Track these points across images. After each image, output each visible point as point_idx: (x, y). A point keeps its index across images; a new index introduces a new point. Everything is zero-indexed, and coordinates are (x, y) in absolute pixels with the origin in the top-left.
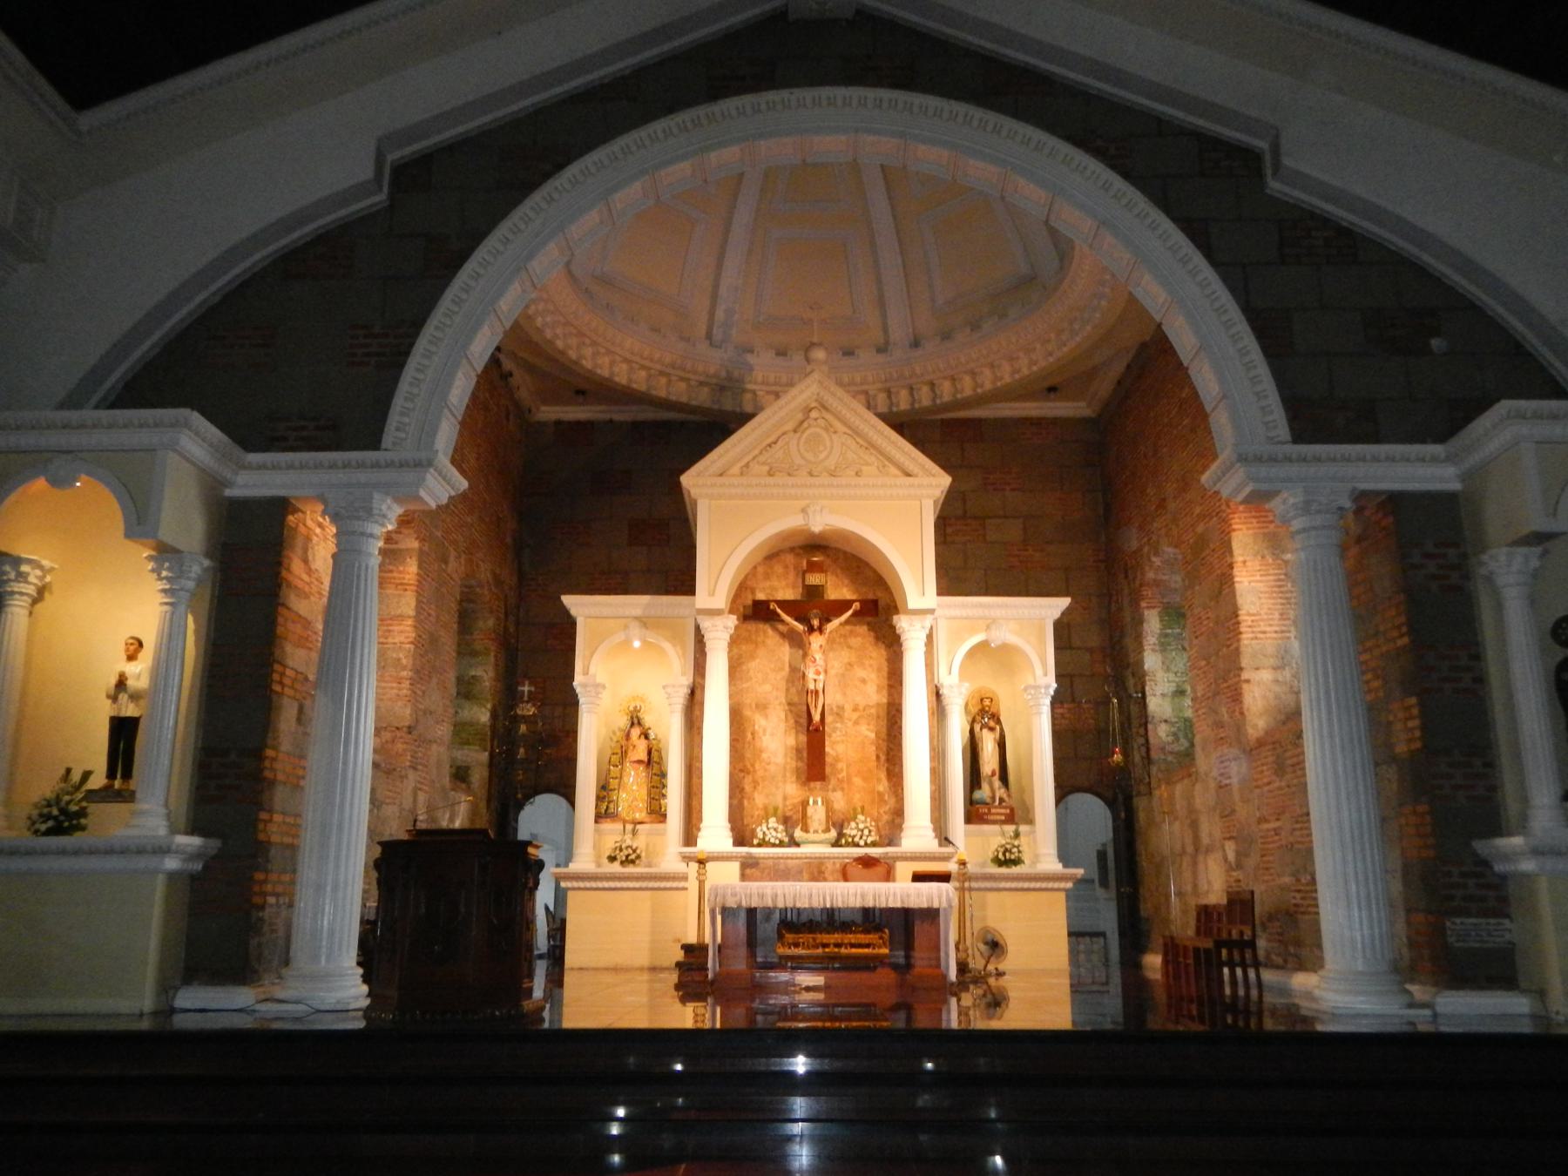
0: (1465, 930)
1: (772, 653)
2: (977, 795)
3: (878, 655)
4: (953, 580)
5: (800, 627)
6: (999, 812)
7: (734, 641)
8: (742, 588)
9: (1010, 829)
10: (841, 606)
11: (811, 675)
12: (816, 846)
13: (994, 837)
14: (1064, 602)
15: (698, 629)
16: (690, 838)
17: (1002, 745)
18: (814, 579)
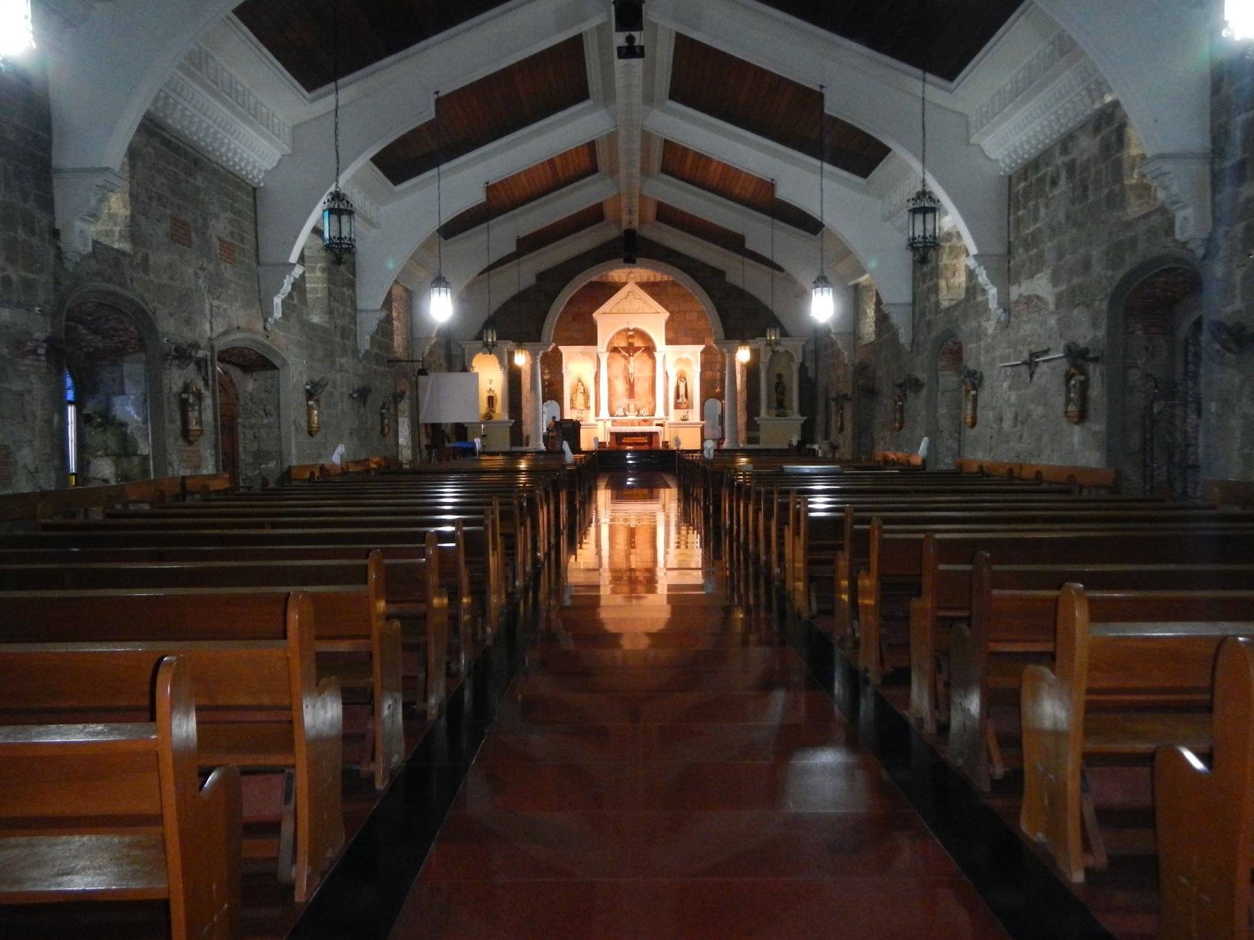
0: (752, 434)
1: (619, 361)
2: (679, 401)
3: (650, 362)
4: (669, 341)
5: (627, 355)
6: (684, 406)
7: (608, 359)
8: (611, 342)
9: (686, 410)
10: (639, 349)
11: (630, 369)
12: (632, 416)
13: (682, 413)
14: (704, 346)
15: (598, 356)
16: (597, 414)
17: (686, 386)
18: (631, 340)
